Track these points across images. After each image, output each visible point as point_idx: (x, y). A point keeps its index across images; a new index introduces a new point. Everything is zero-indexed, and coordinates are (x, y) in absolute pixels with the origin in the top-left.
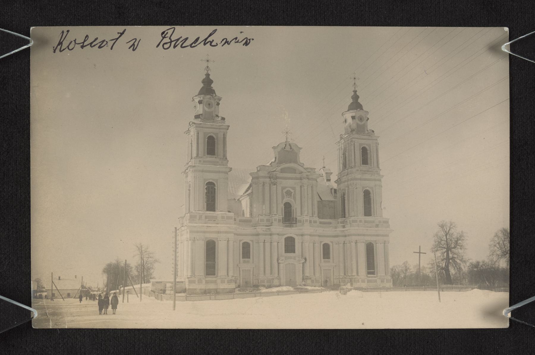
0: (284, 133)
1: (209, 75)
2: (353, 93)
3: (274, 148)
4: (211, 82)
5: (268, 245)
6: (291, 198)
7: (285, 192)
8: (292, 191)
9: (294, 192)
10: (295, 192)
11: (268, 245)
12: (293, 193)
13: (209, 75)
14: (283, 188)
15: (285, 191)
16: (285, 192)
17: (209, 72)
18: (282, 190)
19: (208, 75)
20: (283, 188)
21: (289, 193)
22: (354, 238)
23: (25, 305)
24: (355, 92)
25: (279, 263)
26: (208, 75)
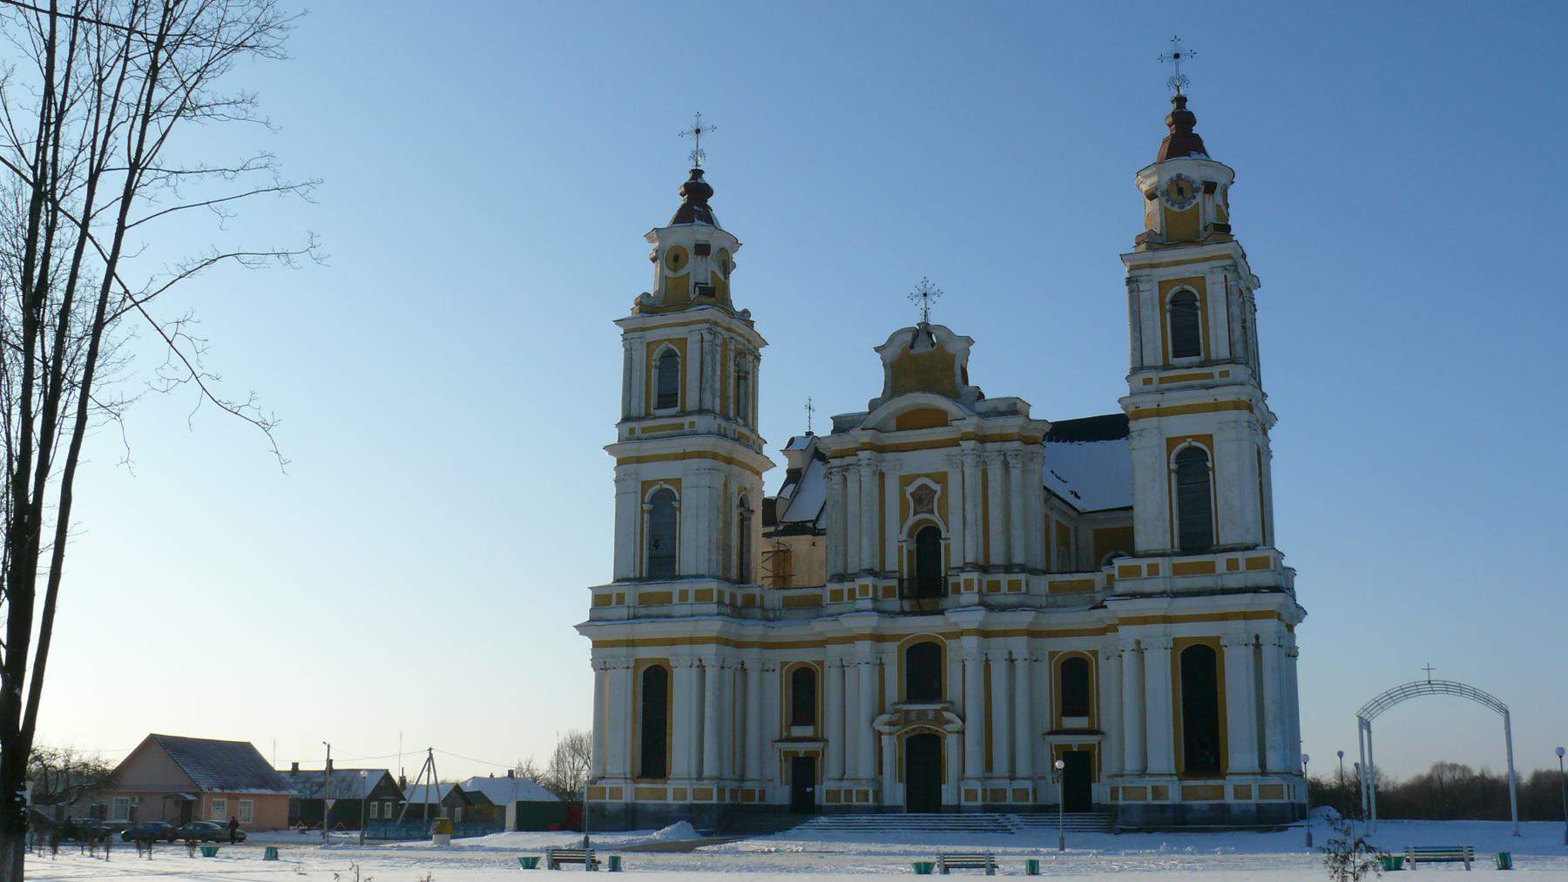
0: (916, 296)
1: (702, 172)
2: (1172, 107)
3: (877, 349)
4: (707, 191)
6: (931, 512)
7: (911, 494)
8: (937, 487)
9: (942, 489)
12: (939, 493)
13: (702, 172)
14: (905, 481)
15: (911, 489)
16: (911, 494)
18: (902, 493)
19: (697, 173)
20: (905, 481)
21: (923, 498)
23: (526, 831)
24: (1181, 101)
25: (878, 735)
26: (697, 173)
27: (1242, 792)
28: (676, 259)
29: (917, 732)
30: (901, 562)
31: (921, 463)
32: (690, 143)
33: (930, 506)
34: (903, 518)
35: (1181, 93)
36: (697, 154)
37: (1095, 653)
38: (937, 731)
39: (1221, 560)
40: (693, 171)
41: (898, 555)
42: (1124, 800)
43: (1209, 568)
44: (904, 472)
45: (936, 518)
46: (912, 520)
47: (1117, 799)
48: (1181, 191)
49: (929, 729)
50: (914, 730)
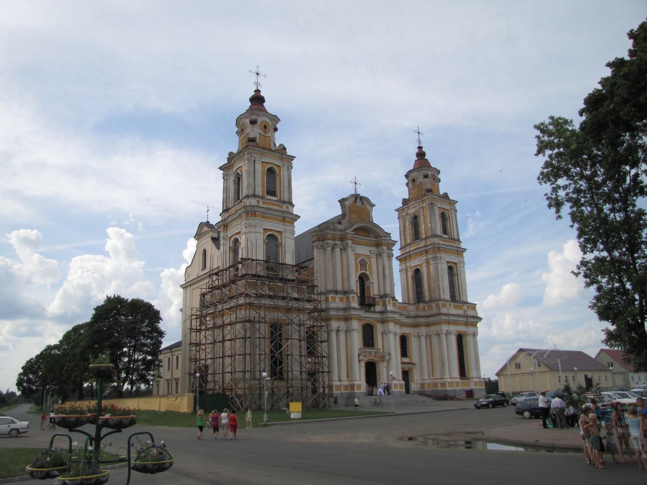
5: (342, 335)
10: (370, 262)
11: (342, 335)
17: (259, 88)
18: (356, 259)
19: (258, 91)
22: (445, 328)
24: (420, 148)
25: (359, 361)
26: (258, 91)
27: (476, 383)
28: (265, 127)
29: (370, 360)
30: (357, 289)
31: (363, 250)
32: (254, 78)
33: (365, 268)
34: (357, 272)
35: (421, 146)
36: (257, 84)
37: (410, 334)
38: (377, 361)
39: (465, 306)
40: (255, 91)
41: (354, 285)
42: (449, 387)
43: (461, 308)
44: (357, 252)
45: (368, 273)
46: (360, 272)
47: (445, 387)
48: (434, 179)
49: (374, 360)
50: (369, 359)
